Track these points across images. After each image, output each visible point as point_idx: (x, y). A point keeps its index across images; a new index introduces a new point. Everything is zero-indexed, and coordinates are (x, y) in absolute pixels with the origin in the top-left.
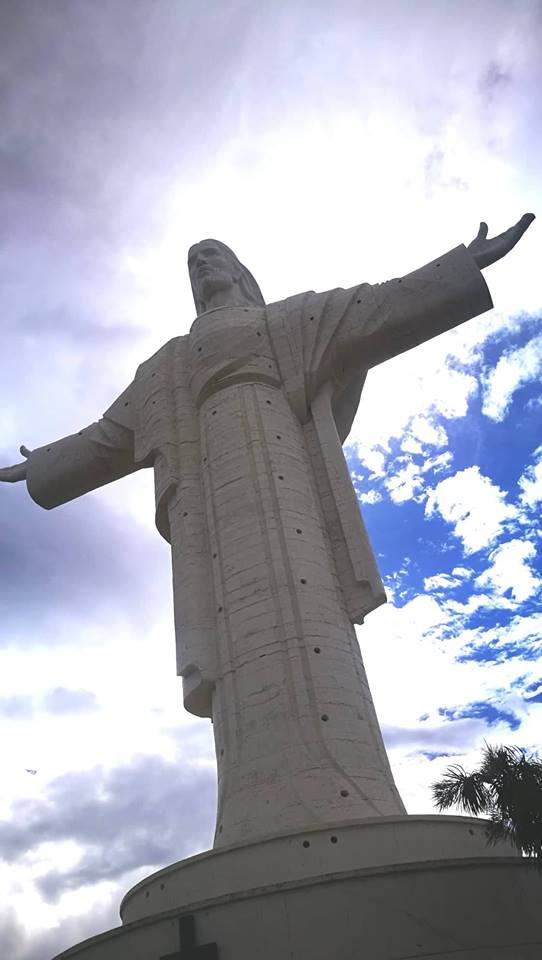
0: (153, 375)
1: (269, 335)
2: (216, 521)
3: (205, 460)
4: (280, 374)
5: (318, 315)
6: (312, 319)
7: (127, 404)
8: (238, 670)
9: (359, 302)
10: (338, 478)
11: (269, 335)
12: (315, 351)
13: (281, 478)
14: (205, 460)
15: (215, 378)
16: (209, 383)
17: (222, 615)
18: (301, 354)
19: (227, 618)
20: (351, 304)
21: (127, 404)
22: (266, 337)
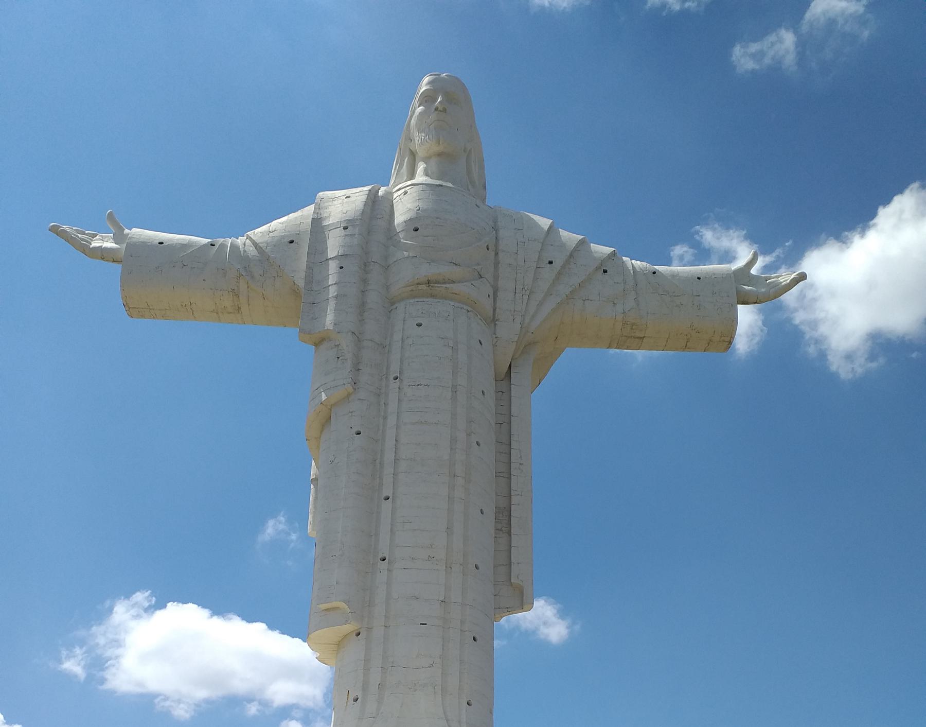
1: (497, 254)
2: (396, 460)
3: (396, 378)
4: (495, 310)
5: (558, 263)
6: (551, 262)
9: (605, 271)
10: (520, 464)
11: (497, 254)
12: (541, 304)
13: (478, 444)
14: (396, 378)
18: (525, 297)
20: (597, 269)
22: (493, 254)
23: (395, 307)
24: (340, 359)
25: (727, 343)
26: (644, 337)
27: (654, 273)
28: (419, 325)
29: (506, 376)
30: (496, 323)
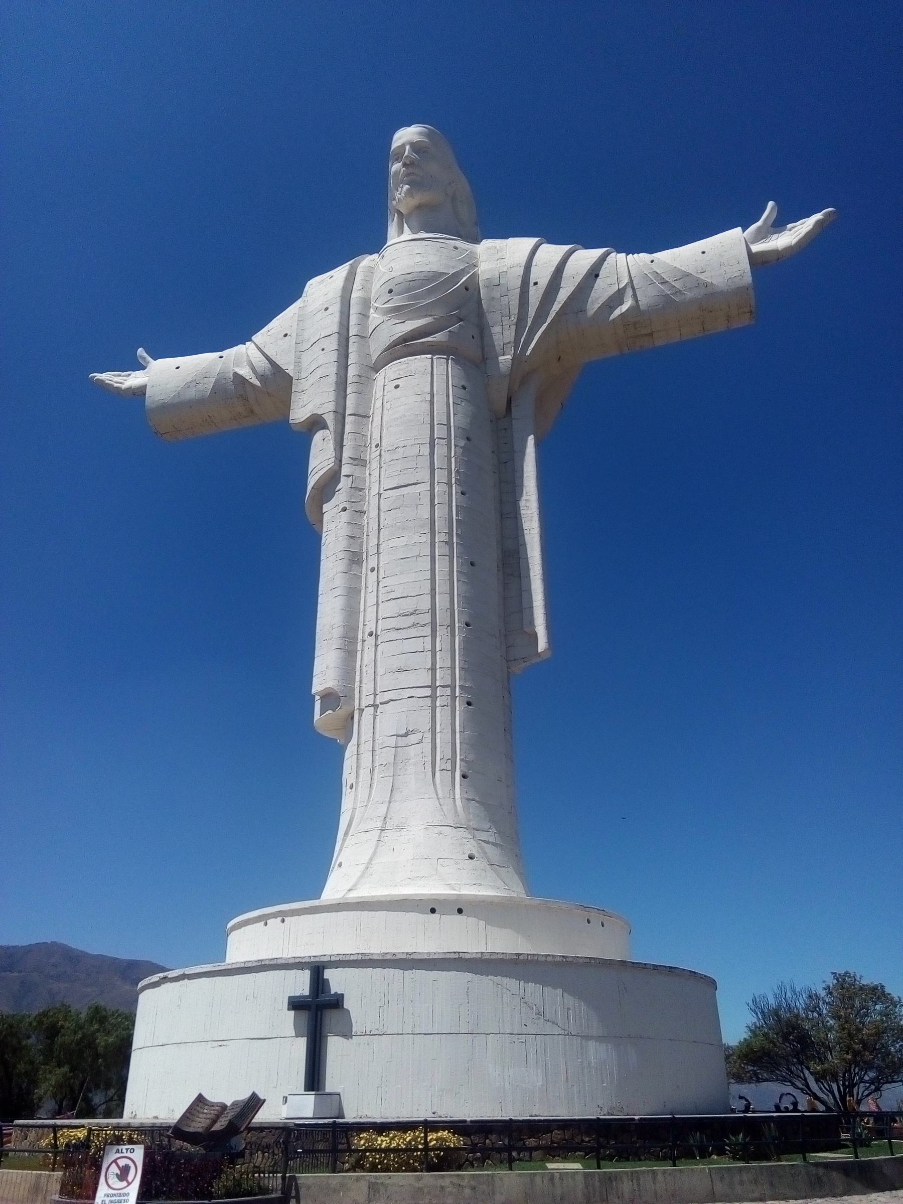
0: (326, 309)
4: (483, 349)
7: (286, 335)
8: (380, 706)
14: (377, 446)
15: (405, 339)
16: (395, 344)
17: (371, 641)
19: (376, 646)
21: (286, 335)
23: (378, 374)
24: (325, 440)
25: (749, 314)
26: (652, 332)
27: (652, 261)
28: (397, 387)
29: (506, 412)
30: (487, 361)
